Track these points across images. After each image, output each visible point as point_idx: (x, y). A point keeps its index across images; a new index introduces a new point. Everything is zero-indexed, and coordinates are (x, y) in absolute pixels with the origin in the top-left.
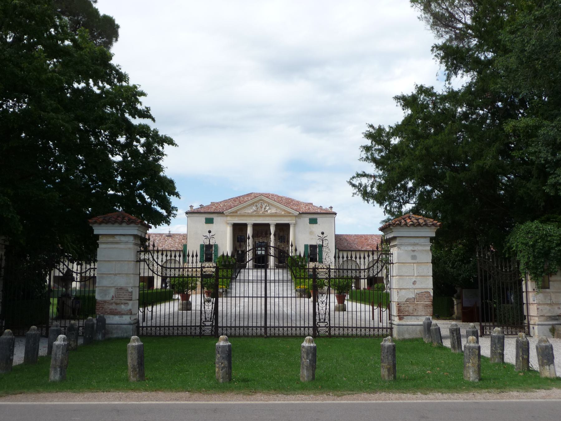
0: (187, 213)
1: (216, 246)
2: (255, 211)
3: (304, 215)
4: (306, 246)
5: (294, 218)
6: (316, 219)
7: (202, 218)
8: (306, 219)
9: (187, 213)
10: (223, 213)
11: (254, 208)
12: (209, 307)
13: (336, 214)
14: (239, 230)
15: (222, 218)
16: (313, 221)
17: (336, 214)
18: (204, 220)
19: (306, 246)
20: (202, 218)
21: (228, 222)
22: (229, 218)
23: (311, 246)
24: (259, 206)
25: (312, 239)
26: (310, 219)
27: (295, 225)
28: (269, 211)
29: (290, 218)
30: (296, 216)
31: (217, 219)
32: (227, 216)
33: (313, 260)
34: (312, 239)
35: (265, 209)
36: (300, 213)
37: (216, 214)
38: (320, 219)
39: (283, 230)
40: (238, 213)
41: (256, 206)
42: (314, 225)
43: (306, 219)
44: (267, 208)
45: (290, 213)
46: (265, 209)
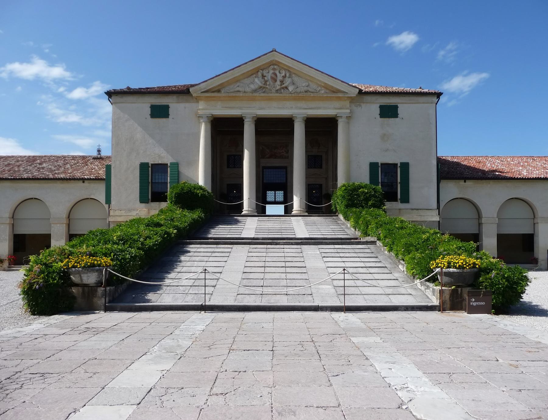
0: (110, 94)
2: (261, 87)
4: (373, 166)
5: (347, 104)
6: (396, 108)
7: (144, 106)
9: (110, 94)
11: (258, 82)
12: (100, 290)
13: (438, 95)
14: (225, 133)
15: (187, 105)
16: (388, 112)
17: (438, 95)
18: (148, 111)
19: (373, 166)
20: (144, 106)
21: (200, 112)
22: (201, 105)
23: (386, 166)
24: (269, 76)
25: (387, 150)
26: (381, 107)
27: (349, 118)
28: (291, 88)
29: (337, 104)
30: (352, 100)
31: (177, 107)
34: (387, 150)
35: (282, 82)
36: (360, 92)
38: (405, 108)
39: (323, 132)
41: (263, 76)
44: (288, 81)
45: (339, 91)
46: (282, 82)
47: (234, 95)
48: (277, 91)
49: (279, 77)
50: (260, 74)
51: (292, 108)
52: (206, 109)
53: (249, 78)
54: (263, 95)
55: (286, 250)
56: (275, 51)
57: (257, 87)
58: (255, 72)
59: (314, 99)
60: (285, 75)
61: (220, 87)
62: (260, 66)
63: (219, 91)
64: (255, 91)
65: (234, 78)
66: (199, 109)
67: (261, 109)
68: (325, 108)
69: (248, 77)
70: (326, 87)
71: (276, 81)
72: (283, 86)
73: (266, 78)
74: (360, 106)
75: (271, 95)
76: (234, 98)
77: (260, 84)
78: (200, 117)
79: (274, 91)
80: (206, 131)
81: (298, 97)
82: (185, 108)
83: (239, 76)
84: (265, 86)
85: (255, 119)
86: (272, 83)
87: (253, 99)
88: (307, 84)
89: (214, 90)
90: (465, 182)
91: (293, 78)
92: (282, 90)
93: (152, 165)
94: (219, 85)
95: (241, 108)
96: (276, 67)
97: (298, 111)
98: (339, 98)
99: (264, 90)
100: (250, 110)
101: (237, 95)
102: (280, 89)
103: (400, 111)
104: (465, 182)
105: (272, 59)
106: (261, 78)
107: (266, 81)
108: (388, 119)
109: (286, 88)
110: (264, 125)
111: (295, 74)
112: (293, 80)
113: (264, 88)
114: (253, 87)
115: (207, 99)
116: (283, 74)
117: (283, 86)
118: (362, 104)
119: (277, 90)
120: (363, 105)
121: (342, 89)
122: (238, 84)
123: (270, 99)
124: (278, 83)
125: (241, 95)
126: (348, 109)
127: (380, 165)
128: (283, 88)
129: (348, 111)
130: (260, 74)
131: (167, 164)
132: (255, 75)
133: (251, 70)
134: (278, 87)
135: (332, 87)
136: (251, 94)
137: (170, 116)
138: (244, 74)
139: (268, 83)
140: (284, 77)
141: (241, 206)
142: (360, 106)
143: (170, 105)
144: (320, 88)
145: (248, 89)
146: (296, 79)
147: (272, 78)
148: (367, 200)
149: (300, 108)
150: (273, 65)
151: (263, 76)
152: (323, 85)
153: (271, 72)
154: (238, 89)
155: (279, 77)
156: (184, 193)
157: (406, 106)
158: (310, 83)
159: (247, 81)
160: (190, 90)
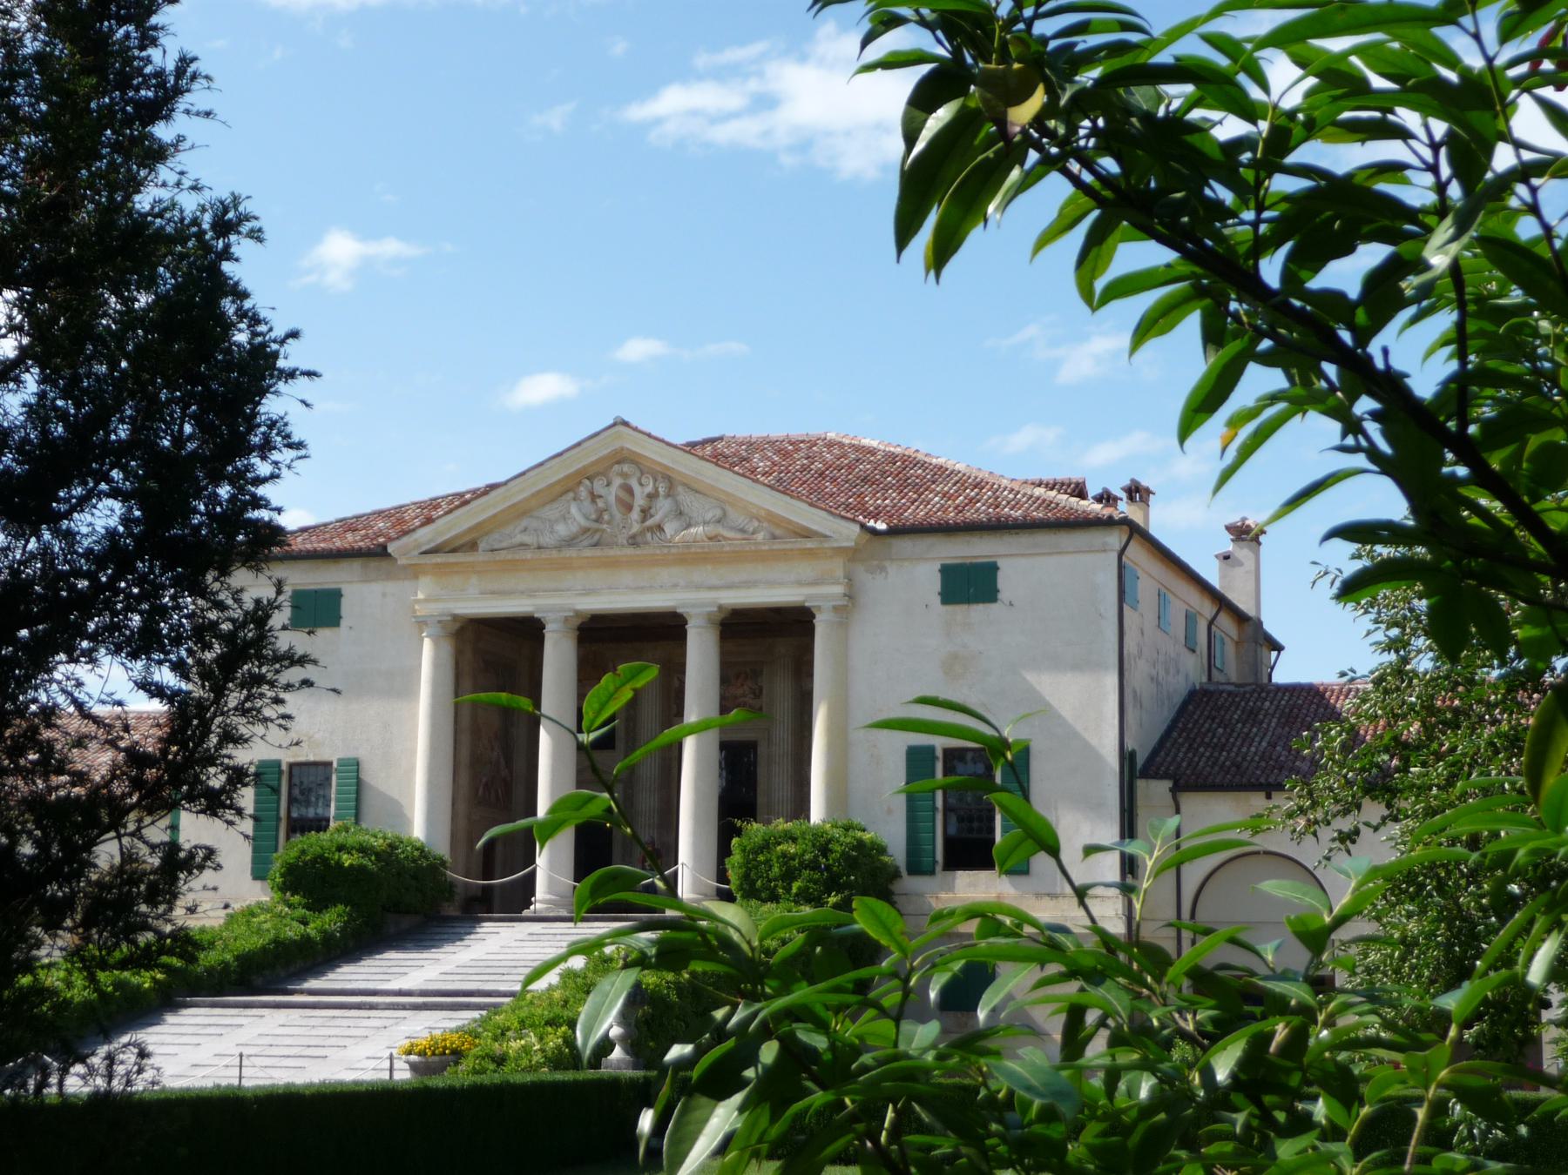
1: (354, 767)
2: (586, 530)
3: (904, 545)
5: (838, 567)
6: (991, 570)
8: (919, 571)
10: (381, 553)
11: (579, 514)
16: (969, 585)
24: (612, 494)
26: (948, 572)
29: (806, 569)
30: (852, 555)
32: (414, 572)
33: (970, 851)
37: (356, 565)
38: (1022, 569)
40: (482, 545)
41: (594, 497)
42: (978, 612)
43: (919, 571)
44: (663, 506)
45: (807, 534)
47: (510, 557)
48: (634, 541)
49: (639, 501)
50: (583, 492)
51: (675, 586)
52: (437, 600)
53: (555, 505)
54: (589, 553)
55: (338, 1022)
56: (626, 424)
57: (574, 529)
58: (567, 487)
59: (737, 557)
60: (656, 489)
61: (474, 535)
62: (584, 468)
63: (472, 546)
64: (570, 542)
65: (514, 505)
66: (418, 601)
67: (588, 592)
68: (771, 584)
69: (553, 500)
70: (772, 519)
71: (630, 508)
72: (649, 522)
73: (600, 503)
74: (883, 569)
75: (611, 552)
76: (512, 566)
77: (583, 522)
78: (422, 623)
79: (622, 539)
80: (436, 665)
81: (690, 557)
82: (384, 595)
83: (526, 499)
84: (595, 525)
85: (577, 622)
86: (618, 516)
87: (566, 566)
88: (718, 513)
89: (457, 543)
90: (1269, 797)
91: (680, 498)
92: (649, 535)
93: (291, 766)
94: (470, 530)
95: (530, 593)
96: (626, 468)
97: (697, 595)
98: (810, 554)
99: (596, 537)
100: (560, 598)
101: (517, 557)
102: (642, 533)
103: (1003, 581)
104: (1269, 797)
105: (617, 445)
106: (587, 504)
107: (600, 512)
108: (964, 607)
109: (660, 528)
110: (607, 639)
111: (685, 485)
112: (676, 502)
113: (597, 531)
114: (562, 530)
115: (440, 570)
116: (649, 489)
117: (649, 522)
118: (887, 564)
119: (633, 537)
120: (892, 568)
121: (815, 527)
122: (524, 523)
123: (614, 564)
124: (635, 515)
125: (529, 556)
126: (837, 583)
127: (939, 753)
128: (650, 529)
129: (838, 590)
130: (583, 492)
131: (330, 764)
132: (571, 495)
133: (559, 482)
134: (636, 528)
135: (790, 522)
136: (555, 554)
137: (343, 622)
138: (538, 492)
139: (606, 517)
140: (652, 496)
141: (527, 888)
142: (883, 569)
143: (346, 590)
144: (756, 524)
145: (547, 540)
146: (684, 497)
147: (618, 499)
148: (789, 876)
149: (698, 587)
150: (618, 462)
151: (594, 497)
152: (763, 513)
153: (617, 482)
154: (520, 538)
155: (639, 501)
156: (306, 863)
157: (1023, 561)
158: (728, 508)
159: (551, 512)
160: (390, 550)
